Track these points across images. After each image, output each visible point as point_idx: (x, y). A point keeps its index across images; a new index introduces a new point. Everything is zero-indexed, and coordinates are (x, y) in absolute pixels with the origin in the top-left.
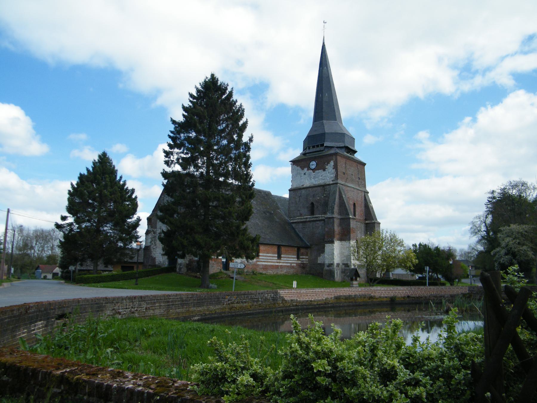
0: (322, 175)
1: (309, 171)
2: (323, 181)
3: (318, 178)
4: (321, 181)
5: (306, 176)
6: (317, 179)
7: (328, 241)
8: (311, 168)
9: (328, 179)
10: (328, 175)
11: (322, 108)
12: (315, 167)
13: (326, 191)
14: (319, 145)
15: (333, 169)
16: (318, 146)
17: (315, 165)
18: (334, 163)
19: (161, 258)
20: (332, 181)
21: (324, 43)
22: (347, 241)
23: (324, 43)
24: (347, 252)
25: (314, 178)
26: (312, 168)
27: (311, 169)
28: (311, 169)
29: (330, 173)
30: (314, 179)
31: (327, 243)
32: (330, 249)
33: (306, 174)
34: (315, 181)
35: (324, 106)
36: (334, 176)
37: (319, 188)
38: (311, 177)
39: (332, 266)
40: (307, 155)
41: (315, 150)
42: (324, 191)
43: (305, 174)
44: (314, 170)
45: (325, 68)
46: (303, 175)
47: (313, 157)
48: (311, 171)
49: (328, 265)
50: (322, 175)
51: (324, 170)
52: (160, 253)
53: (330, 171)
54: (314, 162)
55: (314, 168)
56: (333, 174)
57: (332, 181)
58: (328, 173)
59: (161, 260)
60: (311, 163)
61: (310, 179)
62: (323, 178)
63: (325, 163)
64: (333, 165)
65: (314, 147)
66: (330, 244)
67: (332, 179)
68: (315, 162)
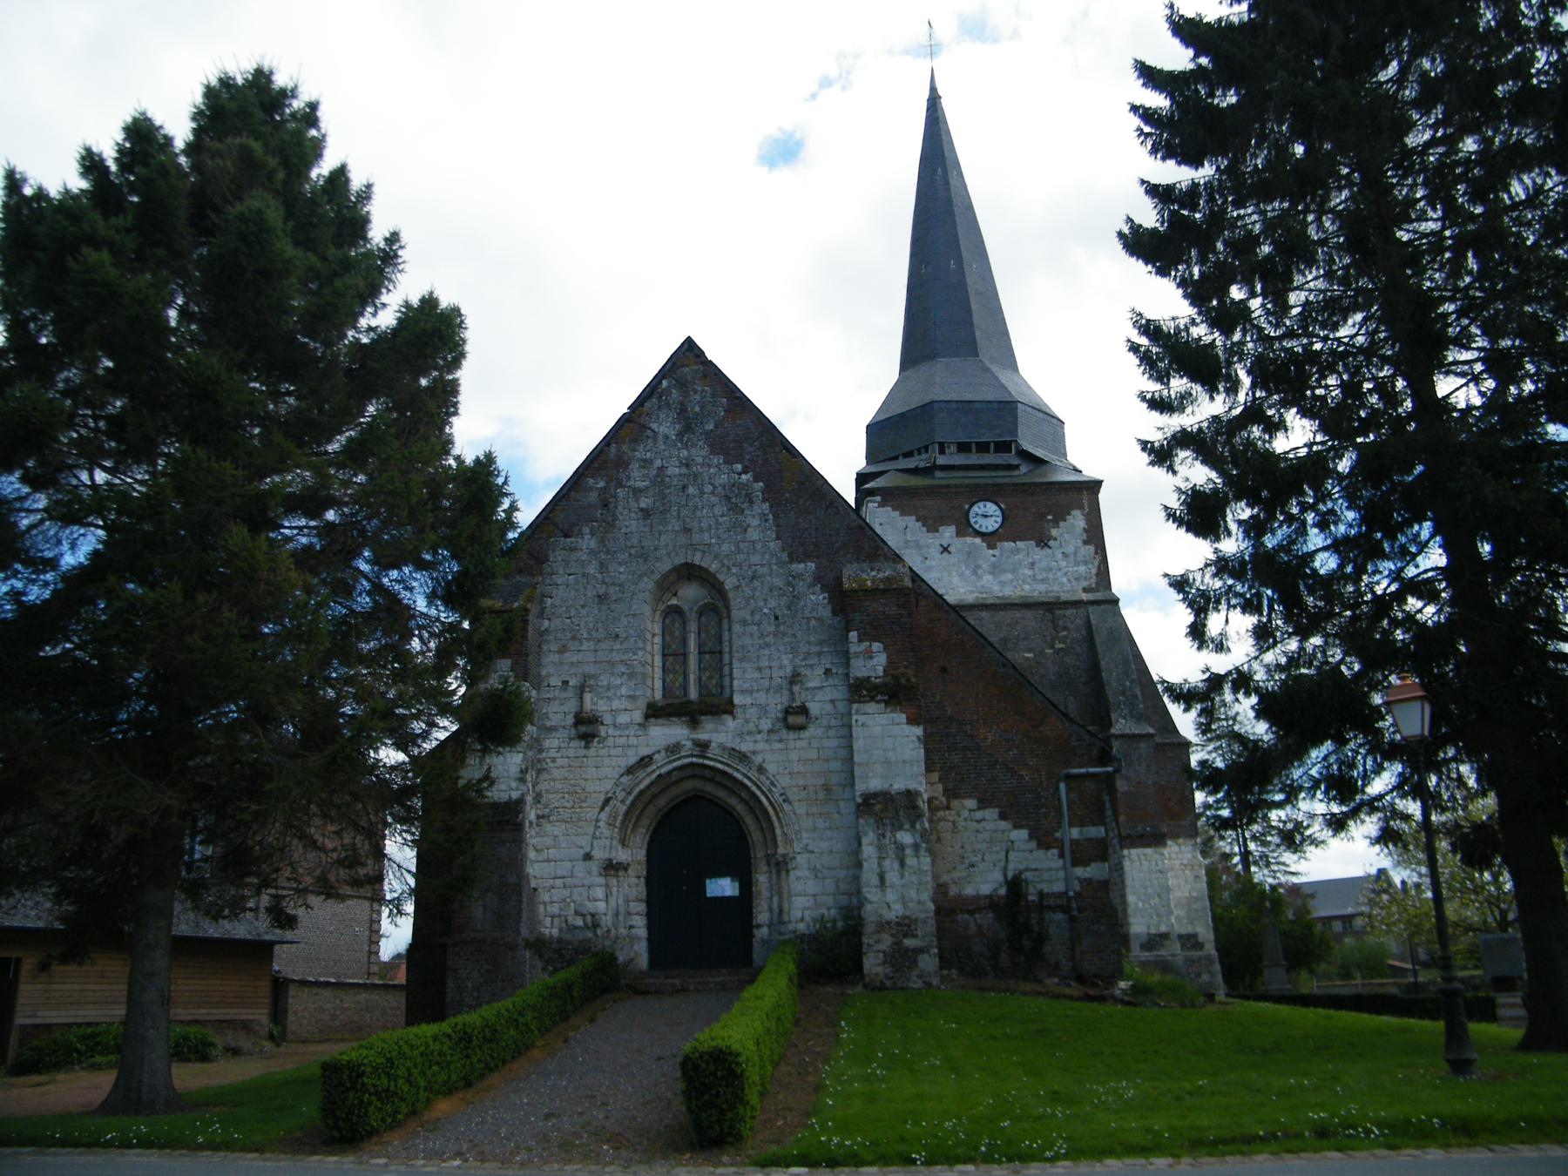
0: (1033, 564)
1: (969, 540)
2: (1043, 587)
3: (1014, 571)
4: (1027, 587)
5: (953, 559)
6: (1010, 576)
7: (1141, 836)
8: (977, 527)
9: (1065, 580)
10: (1064, 564)
11: (969, 311)
12: (996, 526)
13: (1065, 628)
14: (988, 443)
15: (1086, 543)
16: (983, 447)
17: (999, 520)
18: (1088, 521)
19: (599, 893)
20: (1085, 590)
21: (933, 89)
22: (1181, 841)
23: (933, 89)
24: (1188, 887)
25: (995, 570)
26: (983, 530)
27: (978, 533)
28: (978, 533)
29: (1072, 558)
30: (992, 573)
31: (1133, 845)
32: (1150, 871)
33: (945, 554)
34: (1002, 584)
35: (974, 306)
36: (1094, 571)
37: (1029, 614)
38: (978, 567)
39: (1166, 943)
40: (938, 474)
41: (973, 459)
42: (1055, 627)
43: (945, 549)
44: (990, 538)
45: (1393, 67)
46: (934, 551)
47: (986, 485)
48: (978, 540)
49: (1145, 939)
50: (1033, 564)
51: (1043, 541)
52: (588, 857)
53: (1070, 549)
54: (989, 505)
55: (991, 529)
56: (1085, 563)
57: (1085, 590)
58: (1060, 556)
59: (601, 906)
60: (975, 508)
61: (975, 573)
62: (1039, 577)
63: (1043, 516)
64: (1085, 530)
65: (963, 448)
66: (1149, 851)
67: (1085, 584)
68: (994, 507)
